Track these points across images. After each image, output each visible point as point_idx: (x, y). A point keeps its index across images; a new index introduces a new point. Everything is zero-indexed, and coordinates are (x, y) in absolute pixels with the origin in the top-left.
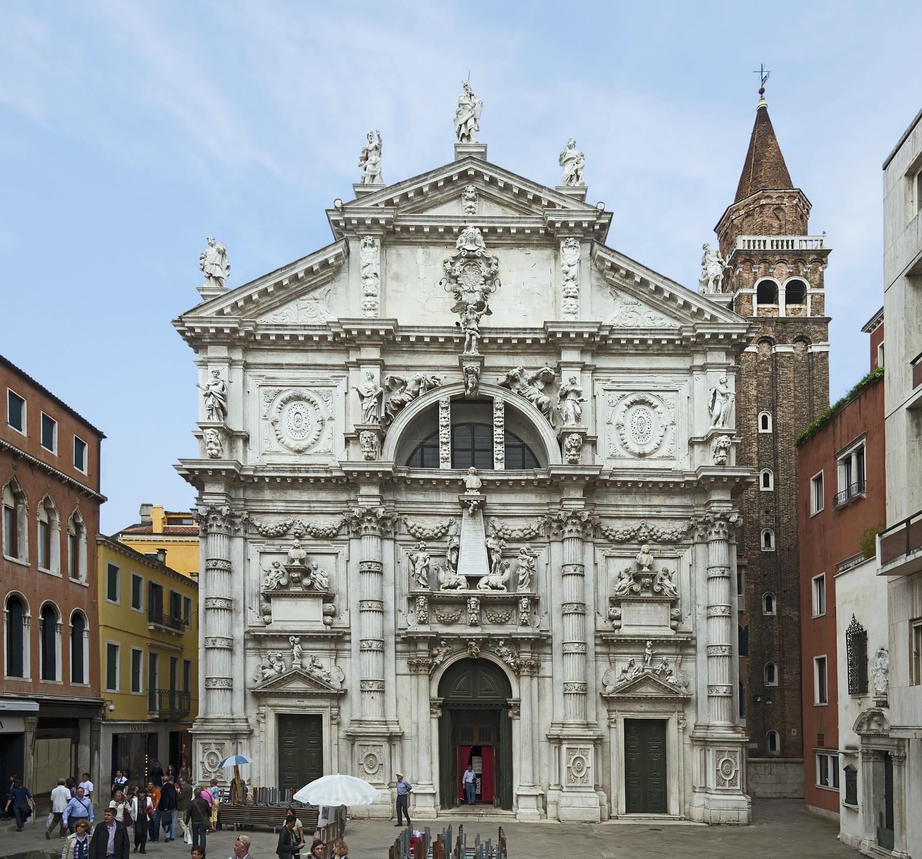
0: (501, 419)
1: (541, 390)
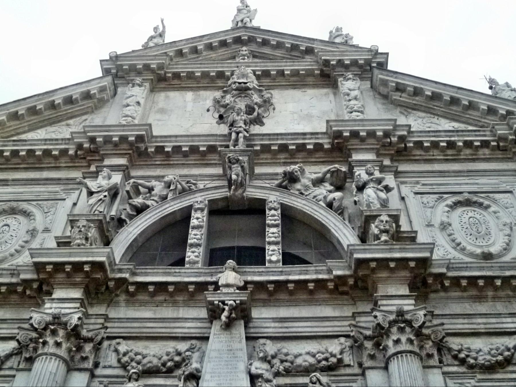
0: (276, 218)
1: (330, 192)
